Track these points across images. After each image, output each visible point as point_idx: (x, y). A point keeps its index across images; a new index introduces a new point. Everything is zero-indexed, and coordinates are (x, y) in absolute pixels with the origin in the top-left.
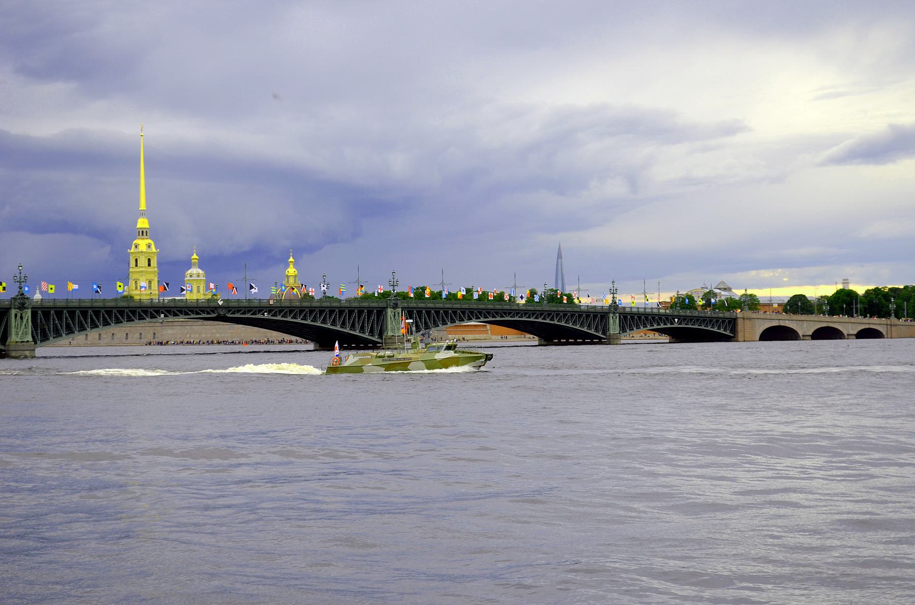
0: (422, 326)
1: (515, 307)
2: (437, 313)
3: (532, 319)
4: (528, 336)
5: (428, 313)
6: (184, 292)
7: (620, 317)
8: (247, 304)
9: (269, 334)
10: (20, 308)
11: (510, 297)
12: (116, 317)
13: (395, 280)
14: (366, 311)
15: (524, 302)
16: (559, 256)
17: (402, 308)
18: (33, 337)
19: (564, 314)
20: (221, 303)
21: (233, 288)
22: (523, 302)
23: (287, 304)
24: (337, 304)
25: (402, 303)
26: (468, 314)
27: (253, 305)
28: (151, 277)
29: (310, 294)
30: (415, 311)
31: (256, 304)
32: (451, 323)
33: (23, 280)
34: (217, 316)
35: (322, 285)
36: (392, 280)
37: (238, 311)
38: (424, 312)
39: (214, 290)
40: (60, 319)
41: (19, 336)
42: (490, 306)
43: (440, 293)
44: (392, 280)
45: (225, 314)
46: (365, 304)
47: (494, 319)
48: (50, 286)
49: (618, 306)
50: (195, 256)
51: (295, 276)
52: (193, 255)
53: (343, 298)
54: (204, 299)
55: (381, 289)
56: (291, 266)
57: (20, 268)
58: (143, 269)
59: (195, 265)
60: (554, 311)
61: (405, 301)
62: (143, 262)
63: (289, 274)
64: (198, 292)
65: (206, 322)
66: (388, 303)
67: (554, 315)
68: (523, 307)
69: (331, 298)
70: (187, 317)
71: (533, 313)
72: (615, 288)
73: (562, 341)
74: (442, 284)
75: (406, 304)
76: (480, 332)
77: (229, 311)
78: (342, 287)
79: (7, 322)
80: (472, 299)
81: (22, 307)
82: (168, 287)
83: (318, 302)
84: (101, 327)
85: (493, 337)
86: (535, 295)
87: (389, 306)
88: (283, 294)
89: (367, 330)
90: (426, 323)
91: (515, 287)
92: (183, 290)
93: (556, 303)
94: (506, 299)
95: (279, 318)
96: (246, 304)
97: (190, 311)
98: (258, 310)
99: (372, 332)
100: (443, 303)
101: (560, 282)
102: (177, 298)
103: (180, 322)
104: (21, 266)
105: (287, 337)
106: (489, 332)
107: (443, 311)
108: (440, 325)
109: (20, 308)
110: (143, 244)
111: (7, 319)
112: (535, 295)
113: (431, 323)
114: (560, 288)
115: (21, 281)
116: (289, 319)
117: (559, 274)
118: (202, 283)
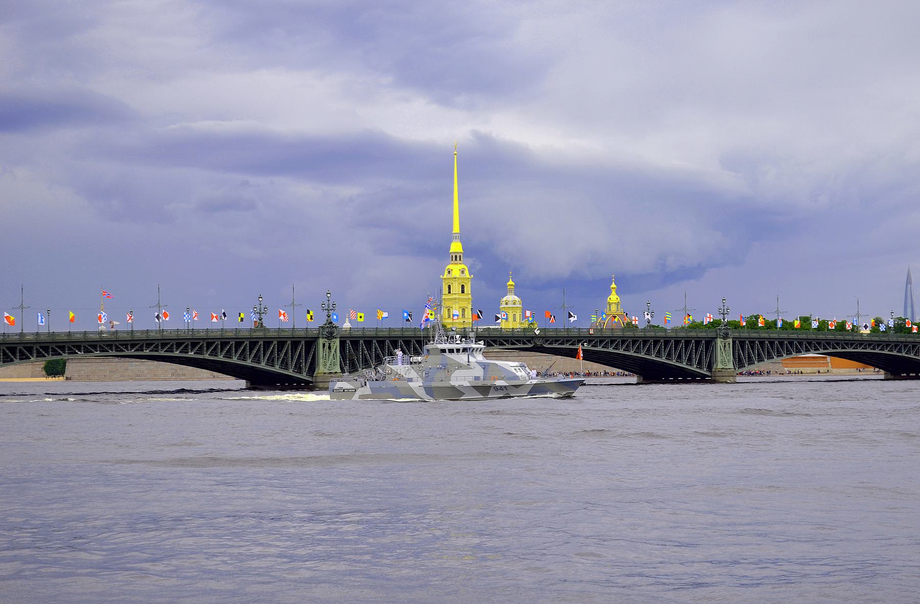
0: (755, 358)
1: (859, 338)
2: (772, 343)
3: (877, 351)
4: (872, 369)
5: (762, 343)
6: (499, 321)
8: (565, 333)
9: (590, 366)
10: (328, 338)
11: (853, 326)
13: (725, 308)
14: (693, 341)
15: (869, 332)
16: (909, 281)
17: (733, 338)
18: (342, 368)
19: (912, 345)
20: (537, 332)
21: (551, 316)
22: (868, 331)
23: (608, 334)
24: (662, 334)
25: (733, 332)
26: (806, 345)
27: (571, 334)
28: (463, 304)
29: (634, 323)
30: (747, 342)
31: (575, 334)
32: (787, 354)
33: (331, 308)
34: (534, 346)
35: (646, 313)
36: (722, 308)
37: (556, 341)
38: (757, 342)
39: (531, 319)
40: (369, 349)
41: (327, 367)
42: (831, 336)
43: (775, 322)
44: (722, 308)
45: (542, 345)
46: (693, 334)
47: (834, 351)
48: (359, 314)
50: (511, 282)
51: (617, 304)
52: (509, 281)
53: (668, 327)
54: (520, 328)
55: (710, 318)
56: (614, 292)
57: (329, 295)
58: (457, 296)
59: (510, 291)
60: (902, 342)
61: (737, 331)
62: (456, 288)
63: (611, 302)
64: (515, 320)
65: (522, 353)
66: (718, 332)
67: (902, 346)
68: (868, 338)
69: (656, 327)
70: (502, 347)
71: (878, 344)
73: (911, 375)
74: (777, 312)
75: (737, 334)
76: (820, 365)
77: (546, 341)
78: (667, 316)
79: (314, 352)
80: (811, 328)
81: (330, 336)
82: (481, 315)
83: (641, 332)
85: (834, 370)
86: (881, 325)
87: (718, 336)
88: (604, 323)
89: (695, 362)
90: (759, 354)
91: (858, 315)
92: (497, 318)
93: (905, 333)
94: (849, 329)
95: (599, 348)
96: (565, 334)
97: (505, 341)
99: (700, 364)
100: (778, 333)
101: (909, 310)
102: (491, 327)
103: (496, 353)
104: (330, 293)
105: (610, 369)
106: (830, 364)
107: (778, 342)
108: (775, 357)
109: (329, 337)
110: (456, 269)
111: (315, 348)
112: (881, 325)
113: (765, 355)
114: (909, 316)
115: (329, 309)
116: (611, 350)
117: (908, 300)
118: (518, 311)
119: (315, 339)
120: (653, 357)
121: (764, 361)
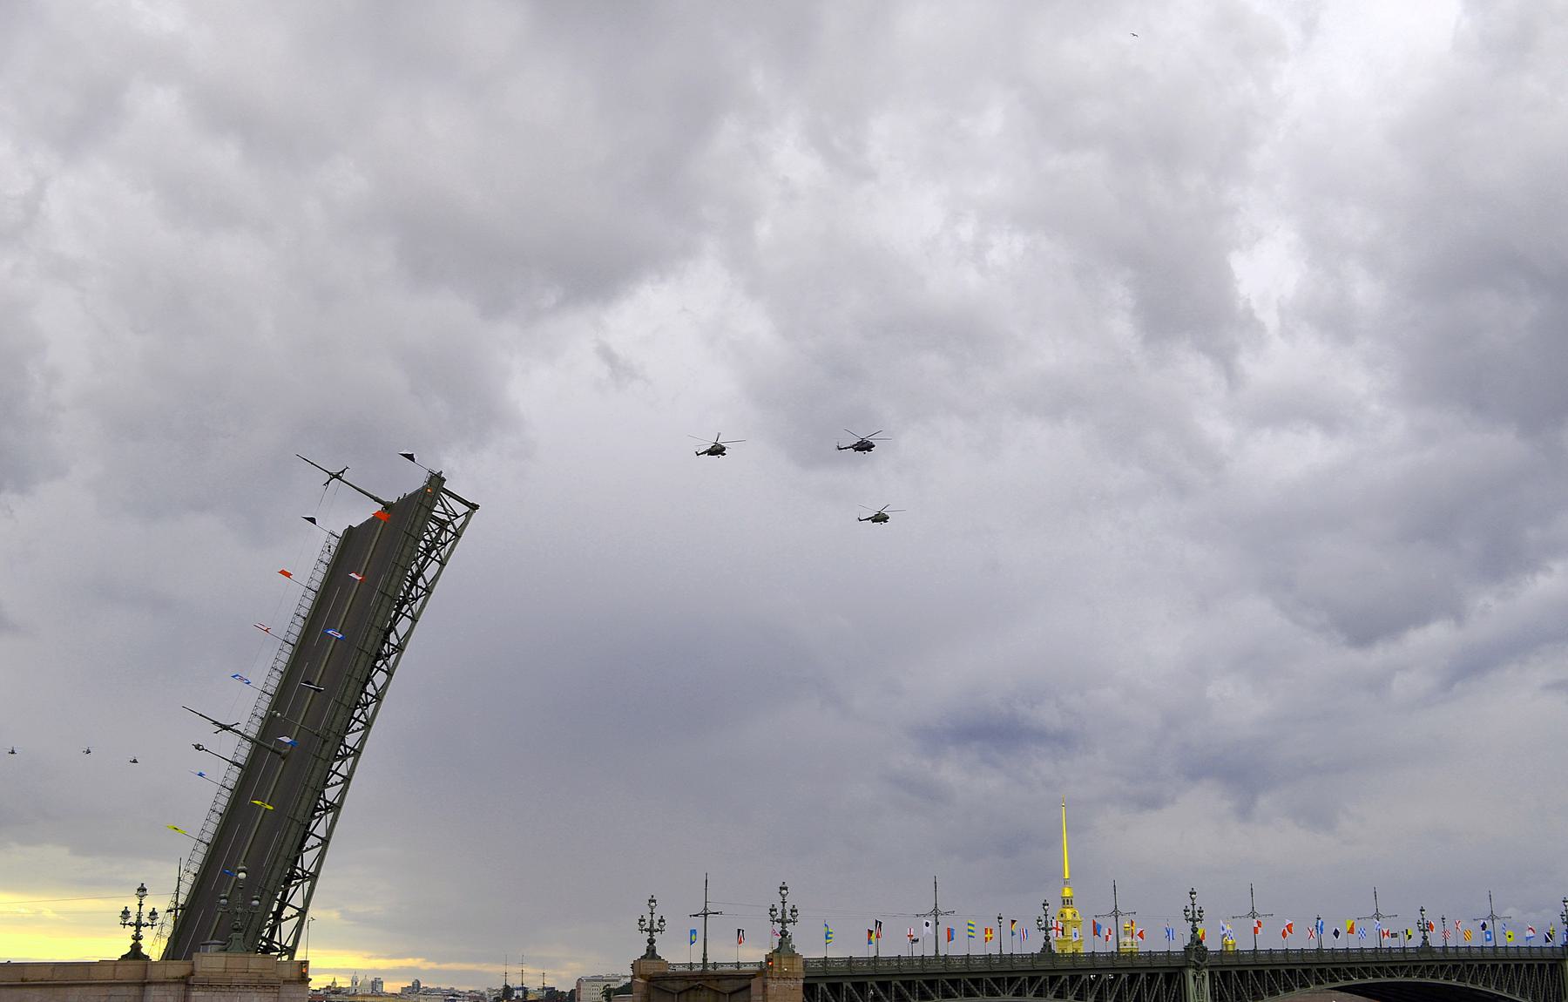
7: (1211, 974)
44: (1190, 908)
49: (1206, 949)
84: (1297, 989)
98: (1427, 966)
119: (1181, 970)
120: (1480, 987)
121: (1263, 999)
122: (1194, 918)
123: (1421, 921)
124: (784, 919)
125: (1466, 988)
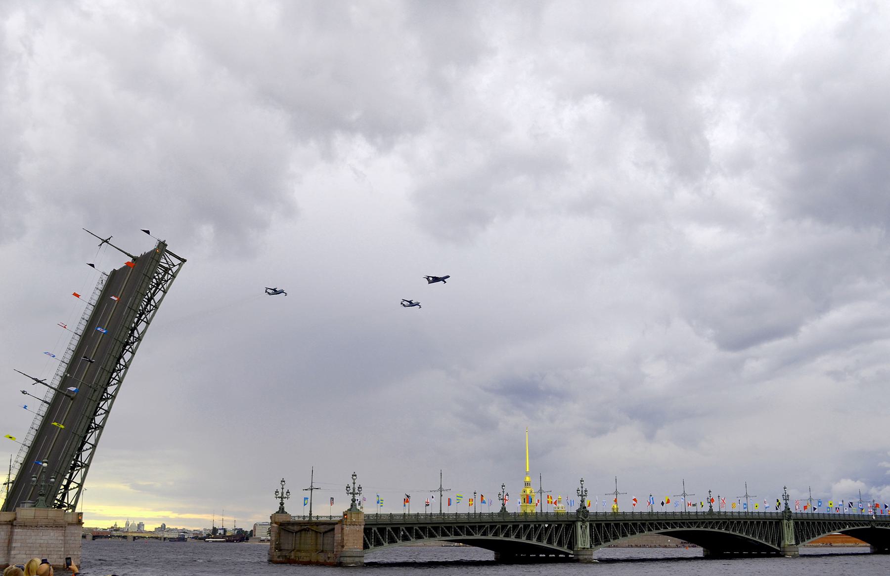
7: (591, 525)
12: (649, 527)
44: (580, 489)
49: (588, 512)
72: (584, 489)
119: (574, 522)
120: (737, 533)
122: (583, 495)
123: (784, 494)
124: (354, 492)
125: (730, 534)
